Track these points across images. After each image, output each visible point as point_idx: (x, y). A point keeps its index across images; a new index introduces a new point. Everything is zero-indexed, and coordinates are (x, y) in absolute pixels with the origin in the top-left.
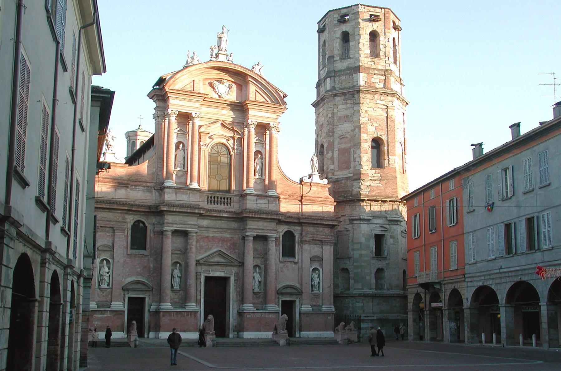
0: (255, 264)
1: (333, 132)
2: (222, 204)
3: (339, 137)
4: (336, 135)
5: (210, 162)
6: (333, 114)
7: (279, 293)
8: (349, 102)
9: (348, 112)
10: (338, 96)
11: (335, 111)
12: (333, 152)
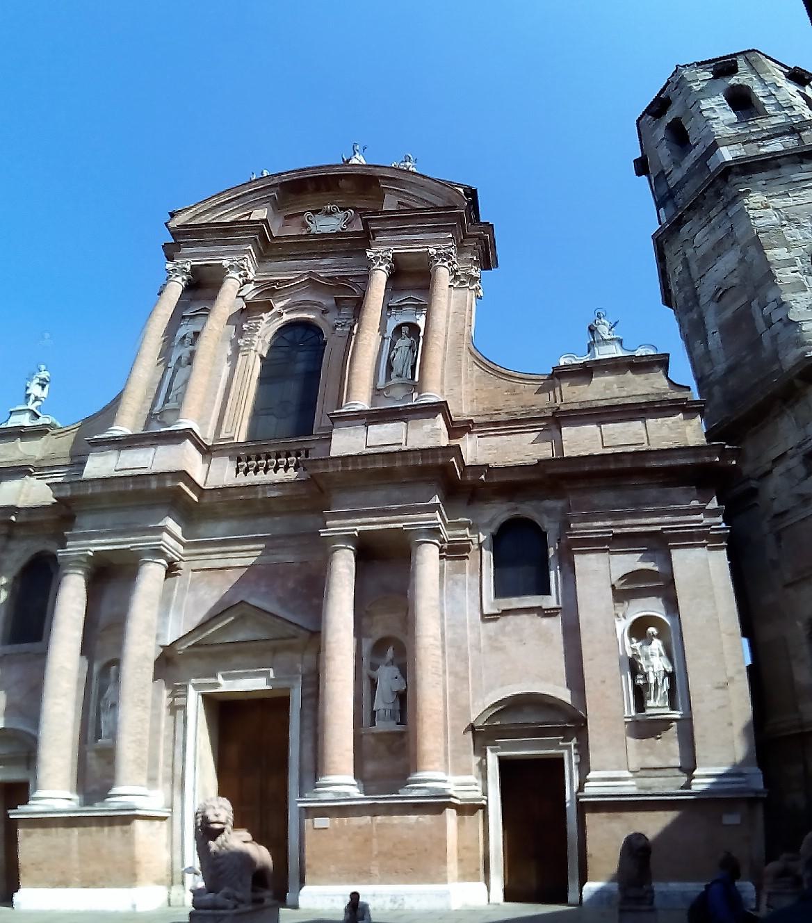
0: (379, 632)
1: (696, 297)
2: (281, 471)
3: (712, 300)
4: (704, 300)
5: (262, 380)
6: (686, 263)
7: (482, 736)
8: (712, 213)
9: (720, 234)
10: (686, 222)
11: (690, 251)
12: (705, 341)
